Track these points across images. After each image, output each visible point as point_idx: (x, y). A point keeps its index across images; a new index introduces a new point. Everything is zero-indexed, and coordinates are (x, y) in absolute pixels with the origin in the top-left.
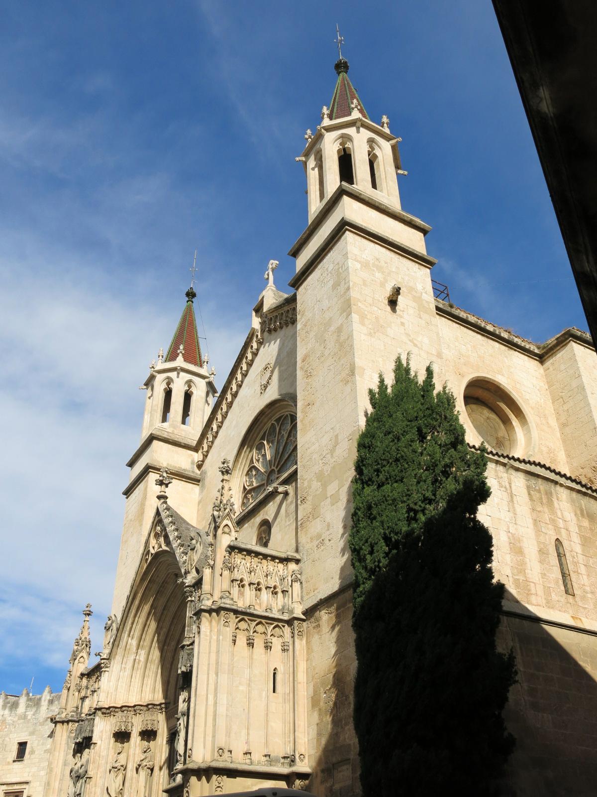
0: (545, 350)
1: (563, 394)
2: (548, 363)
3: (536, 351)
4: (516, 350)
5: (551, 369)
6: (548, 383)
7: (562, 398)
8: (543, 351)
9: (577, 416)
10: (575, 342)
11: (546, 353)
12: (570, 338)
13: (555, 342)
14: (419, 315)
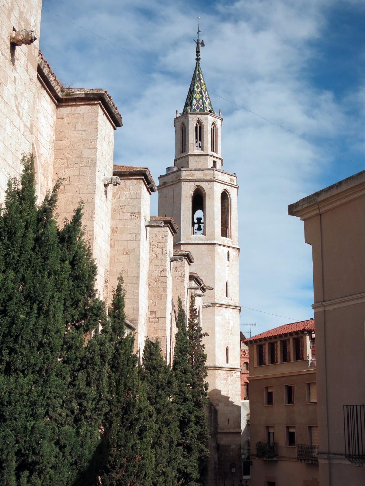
0: (68, 97)
1: (70, 156)
2: (66, 110)
3: (60, 94)
4: (45, 89)
5: (66, 120)
6: (56, 134)
7: (67, 160)
8: (64, 97)
9: (77, 189)
10: (101, 106)
11: (67, 100)
12: (100, 102)
13: (83, 96)
14: (27, 66)
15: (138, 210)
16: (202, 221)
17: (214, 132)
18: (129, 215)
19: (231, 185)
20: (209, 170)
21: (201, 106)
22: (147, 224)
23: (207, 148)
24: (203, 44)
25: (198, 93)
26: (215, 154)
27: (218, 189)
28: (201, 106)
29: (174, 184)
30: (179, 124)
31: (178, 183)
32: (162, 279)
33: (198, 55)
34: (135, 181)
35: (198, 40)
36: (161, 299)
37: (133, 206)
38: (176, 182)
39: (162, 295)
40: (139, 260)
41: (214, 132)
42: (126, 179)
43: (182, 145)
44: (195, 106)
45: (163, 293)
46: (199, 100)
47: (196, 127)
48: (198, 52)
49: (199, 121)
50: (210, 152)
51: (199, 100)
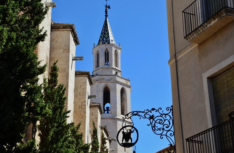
15: (68, 47)
16: (109, 109)
17: (116, 54)
18: (62, 50)
19: (127, 86)
20: (113, 75)
21: (108, 41)
22: (74, 58)
23: (112, 64)
24: (109, 7)
25: (106, 34)
26: (117, 68)
27: (119, 87)
28: (108, 41)
30: (95, 52)
32: (83, 107)
33: (106, 13)
34: (66, 32)
35: (106, 5)
36: (83, 118)
37: (65, 46)
39: (83, 116)
40: (68, 75)
41: (116, 54)
42: (60, 31)
44: (104, 41)
45: (84, 115)
46: (107, 38)
47: (106, 53)
48: (106, 11)
50: (114, 67)
51: (107, 38)
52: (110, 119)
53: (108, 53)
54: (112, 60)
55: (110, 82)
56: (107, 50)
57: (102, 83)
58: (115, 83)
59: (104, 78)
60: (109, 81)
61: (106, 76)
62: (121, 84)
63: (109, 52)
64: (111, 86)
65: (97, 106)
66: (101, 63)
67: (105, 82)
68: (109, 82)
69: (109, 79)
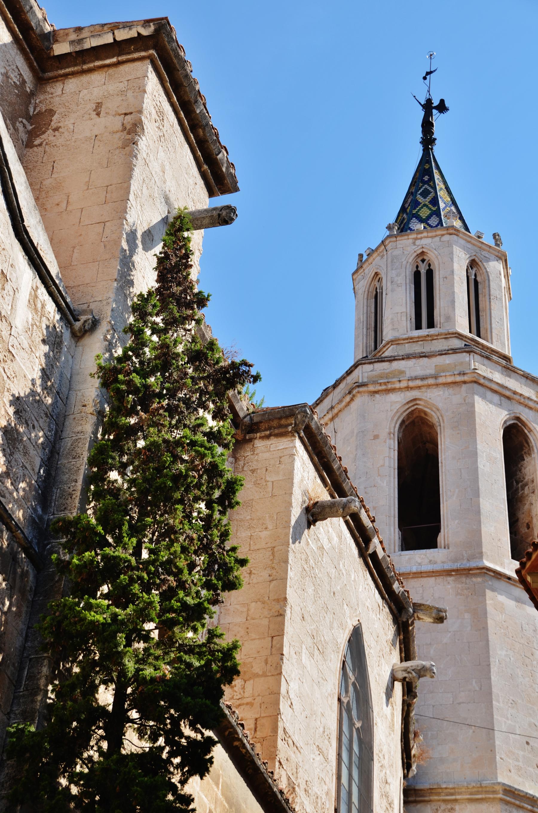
24: (442, 107)
25: (425, 205)
27: (491, 418)
29: (337, 415)
30: (363, 285)
31: (348, 404)
38: (344, 404)
43: (373, 334)
46: (429, 217)
47: (417, 275)
48: (427, 126)
49: (422, 256)
51: (429, 217)
52: (448, 573)
53: (430, 273)
54: (453, 302)
55: (437, 385)
56: (423, 261)
57: (393, 397)
58: (464, 387)
59: (402, 372)
60: (431, 381)
61: (411, 363)
62: (505, 396)
63: (436, 267)
64: (440, 405)
65: (139, 42)
66: (392, 323)
67: (408, 388)
68: (429, 386)
69: (431, 371)
